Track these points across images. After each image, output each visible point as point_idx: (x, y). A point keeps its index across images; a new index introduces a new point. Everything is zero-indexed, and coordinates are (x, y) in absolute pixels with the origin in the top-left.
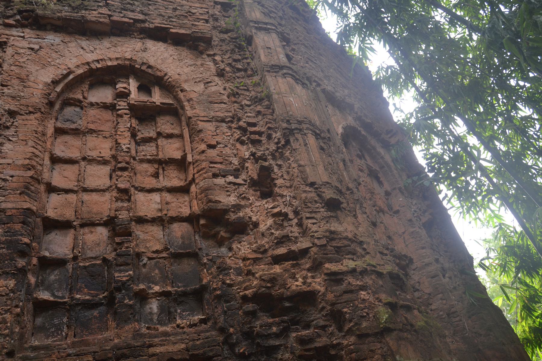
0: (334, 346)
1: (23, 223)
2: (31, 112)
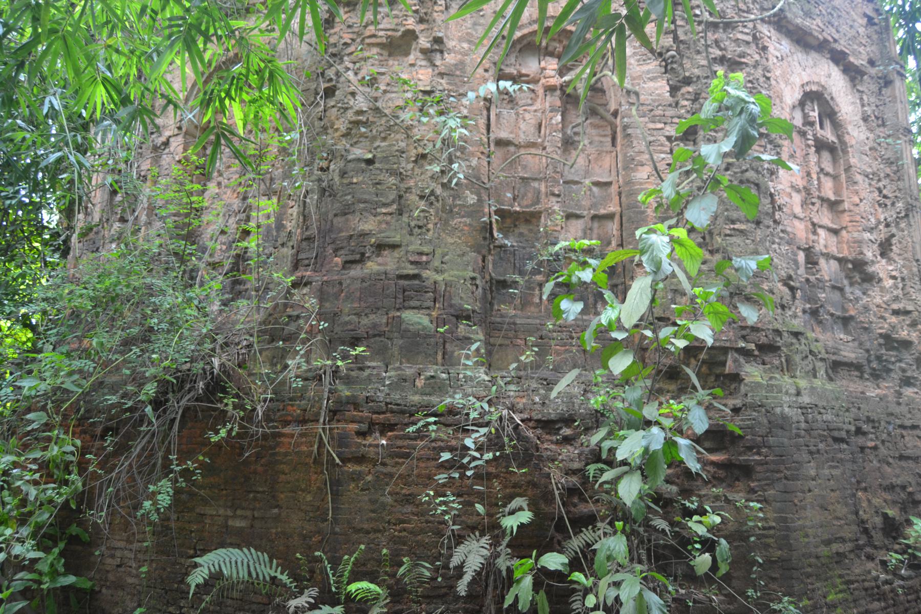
0: (914, 378)
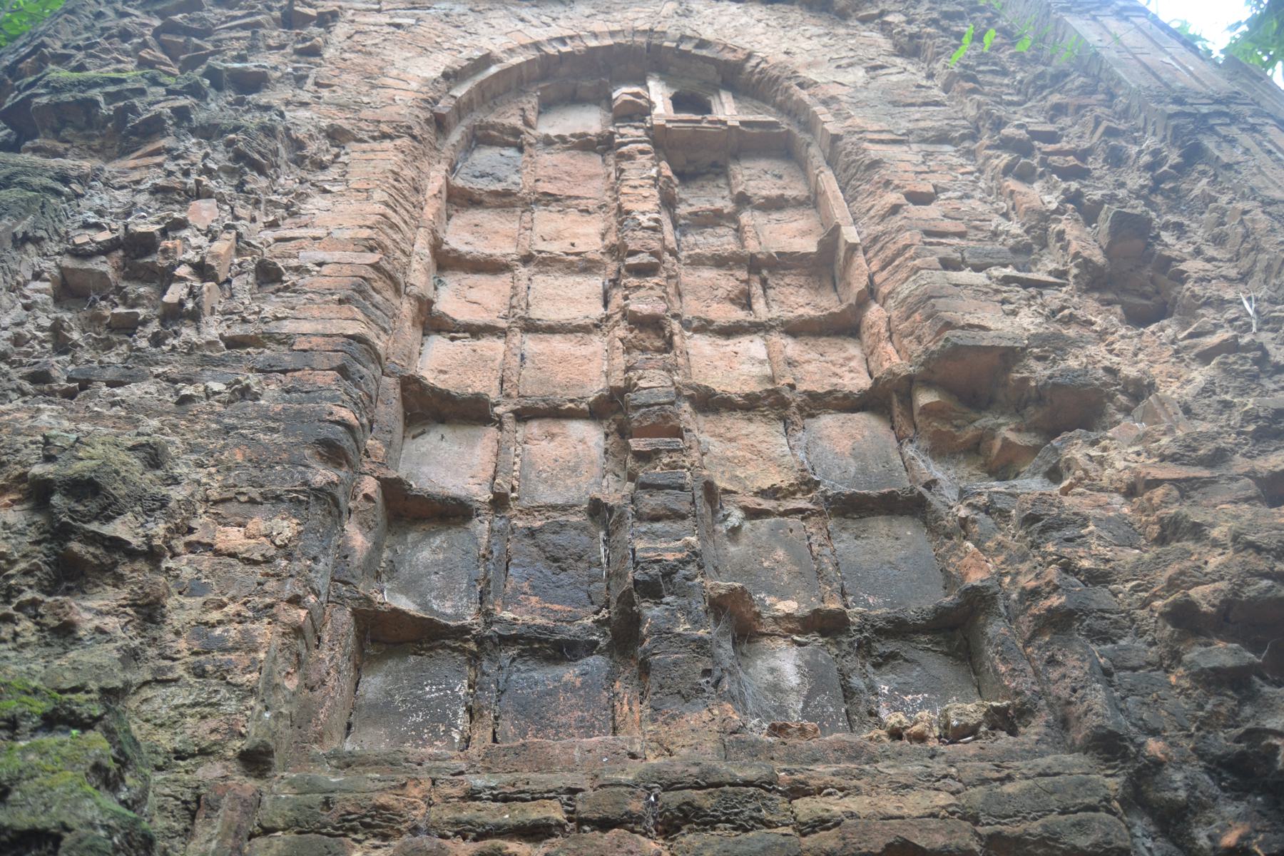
1: (343, 371)
2: (385, 136)
